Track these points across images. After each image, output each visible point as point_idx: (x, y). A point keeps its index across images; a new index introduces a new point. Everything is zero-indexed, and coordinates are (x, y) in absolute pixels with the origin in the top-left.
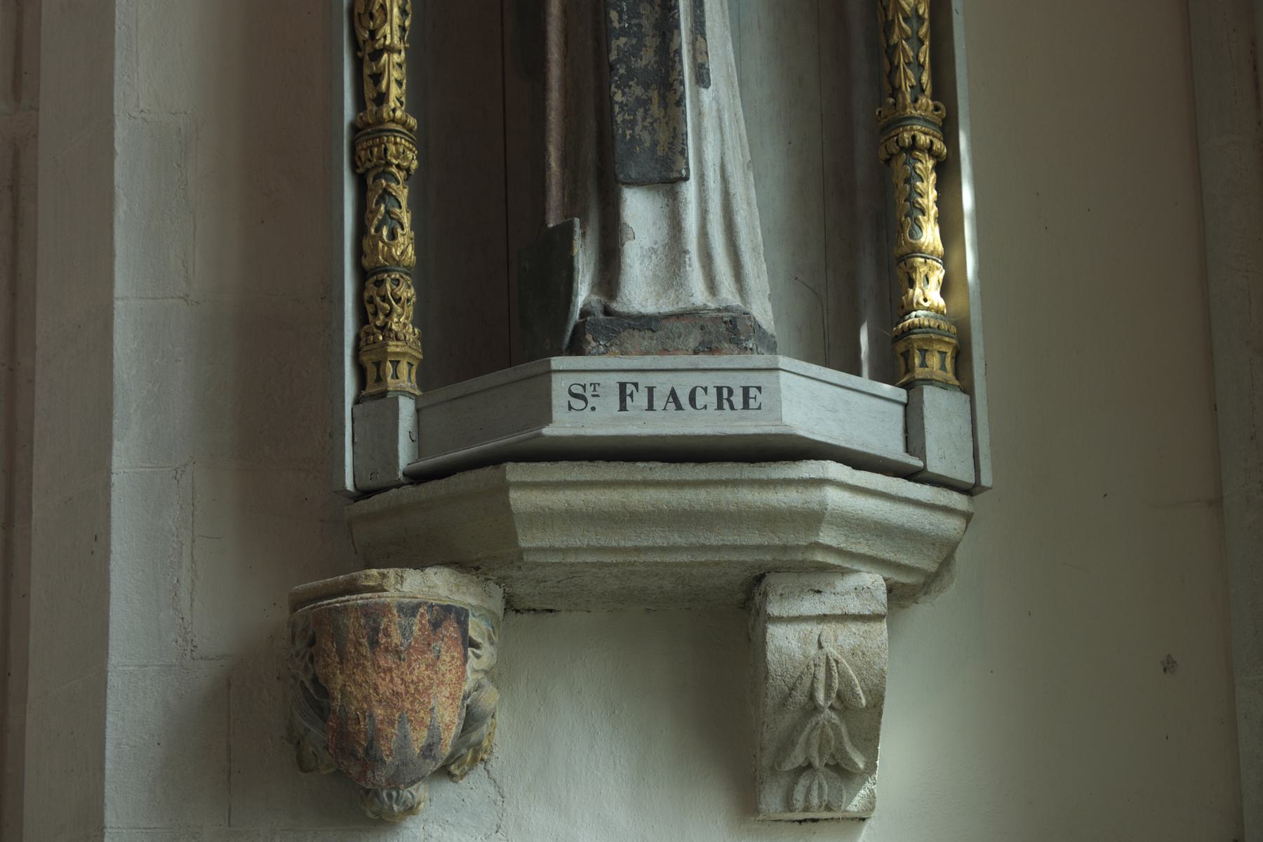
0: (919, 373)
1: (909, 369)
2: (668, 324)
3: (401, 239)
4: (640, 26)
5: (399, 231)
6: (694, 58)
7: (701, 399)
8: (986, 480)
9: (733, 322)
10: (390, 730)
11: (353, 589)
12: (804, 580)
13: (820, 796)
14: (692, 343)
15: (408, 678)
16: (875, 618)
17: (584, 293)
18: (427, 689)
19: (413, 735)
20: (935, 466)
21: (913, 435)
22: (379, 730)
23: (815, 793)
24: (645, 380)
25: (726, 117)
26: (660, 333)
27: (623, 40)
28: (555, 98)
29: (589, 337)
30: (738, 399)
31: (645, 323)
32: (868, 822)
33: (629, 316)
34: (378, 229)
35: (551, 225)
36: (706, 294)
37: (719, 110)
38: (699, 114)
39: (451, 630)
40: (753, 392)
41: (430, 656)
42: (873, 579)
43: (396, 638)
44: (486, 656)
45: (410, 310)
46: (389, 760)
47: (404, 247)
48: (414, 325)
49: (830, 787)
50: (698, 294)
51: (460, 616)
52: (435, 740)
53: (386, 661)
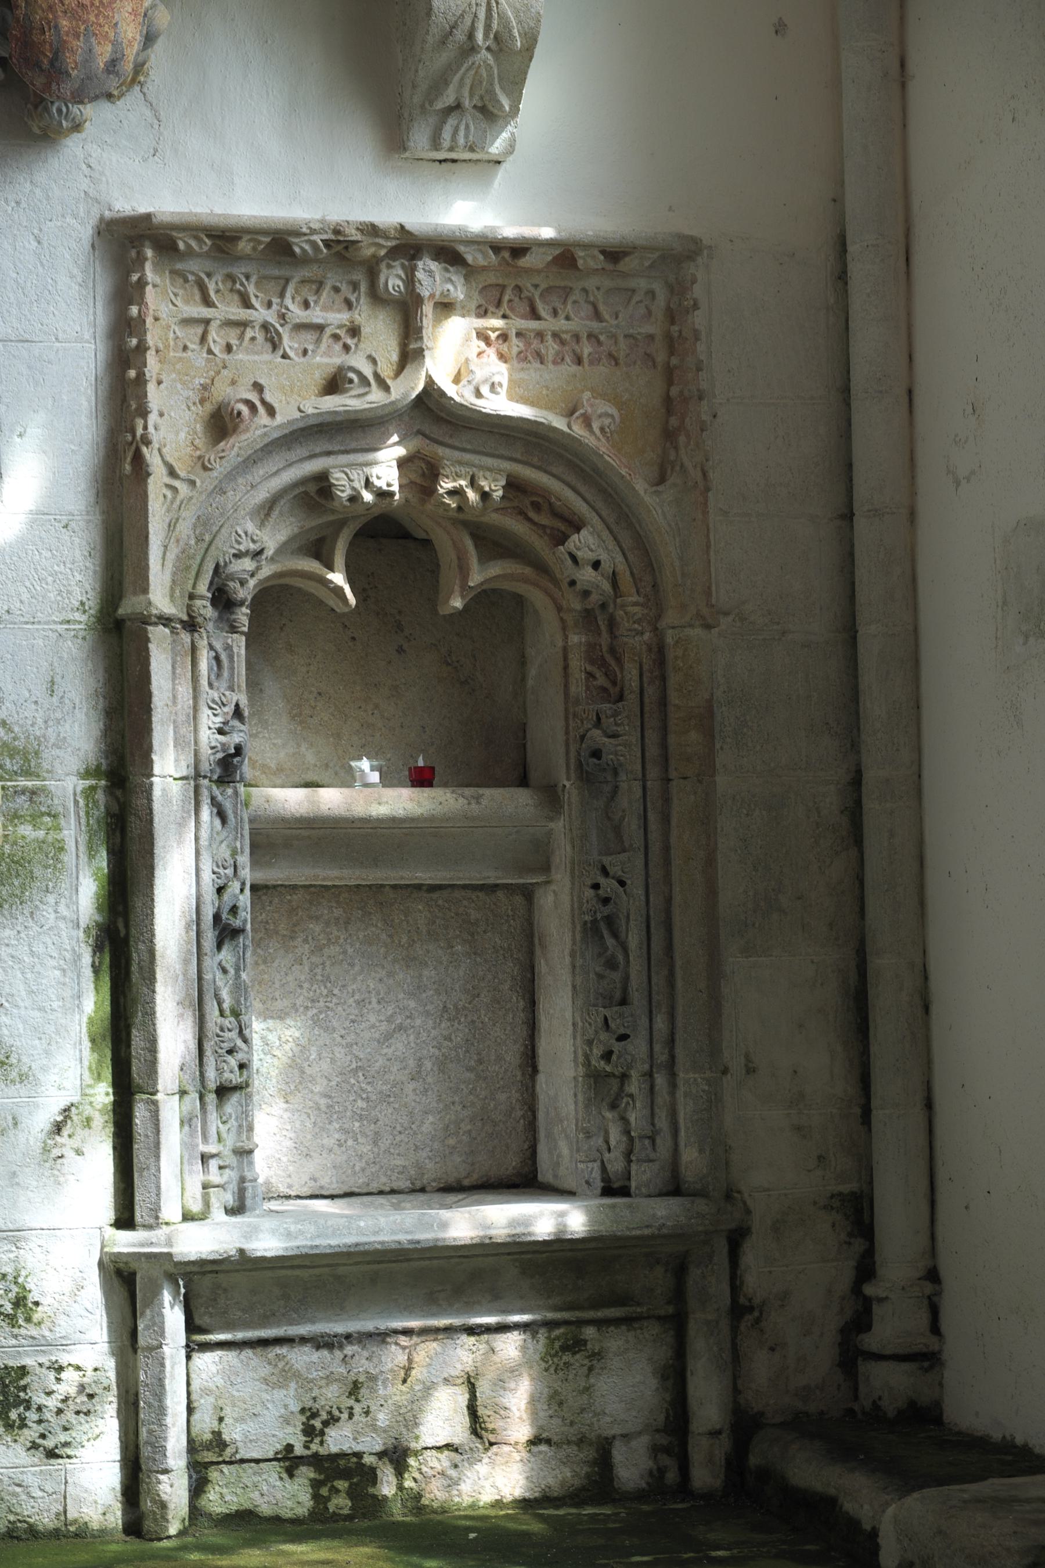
10: (75, 43)
13: (466, 136)
19: (98, 49)
22: (65, 42)
23: (462, 133)
49: (475, 128)
52: (119, 55)
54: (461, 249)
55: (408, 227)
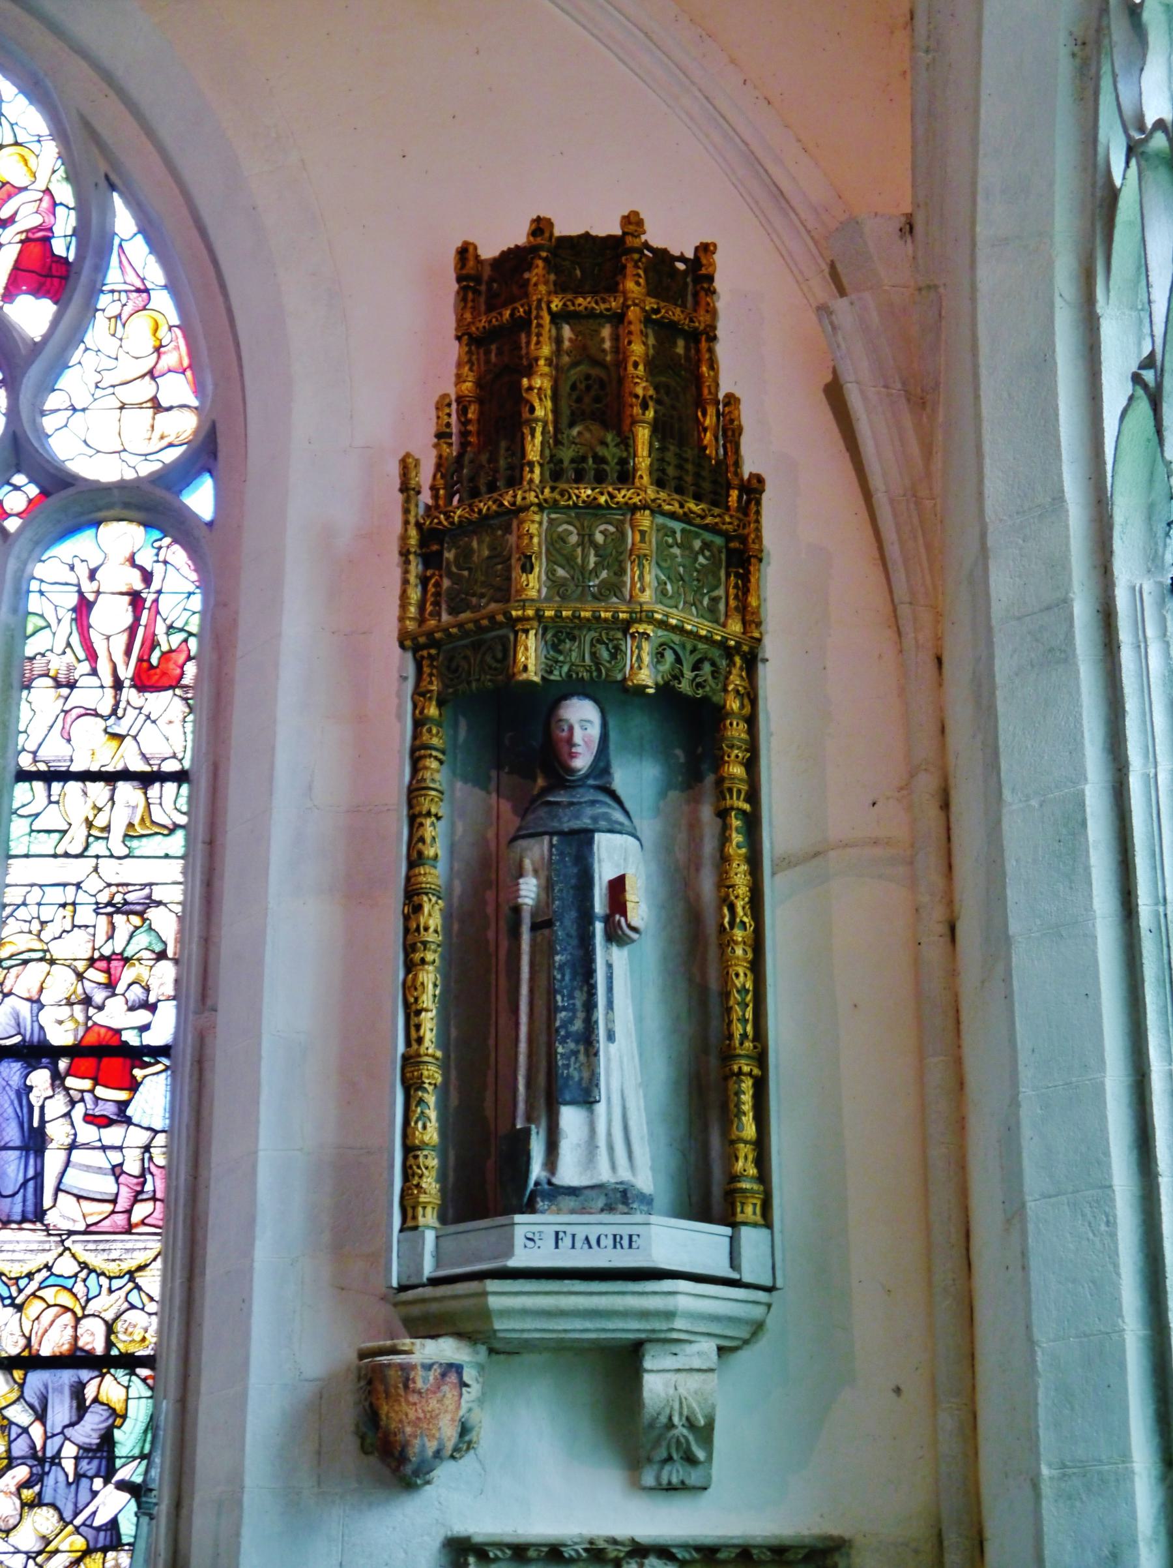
0: (740, 1217)
1: (734, 1214)
2: (587, 1192)
3: (429, 1129)
4: (574, 1004)
5: (428, 1124)
6: (607, 1025)
7: (603, 1242)
8: (779, 1284)
9: (624, 1193)
11: (394, 1351)
12: (667, 1346)
14: (600, 1203)
15: (427, 1409)
16: (711, 1370)
17: (537, 1171)
18: (438, 1415)
19: (428, 1444)
20: (747, 1278)
21: (734, 1259)
24: (570, 1230)
25: (625, 1060)
26: (581, 1198)
27: (563, 1014)
28: (523, 1046)
29: (539, 1199)
30: (625, 1242)
31: (573, 1191)
32: (710, 1491)
33: (562, 1187)
34: (416, 1123)
35: (519, 1126)
36: (610, 1171)
37: (621, 1057)
38: (608, 1060)
39: (453, 1378)
40: (635, 1238)
41: (439, 1395)
42: (709, 1347)
43: (419, 1384)
44: (474, 1390)
45: (434, 1173)
46: (414, 1459)
47: (431, 1134)
48: (437, 1181)
50: (604, 1175)
51: (458, 1368)
53: (414, 1398)
54: (674, 1550)
55: (637, 1539)
